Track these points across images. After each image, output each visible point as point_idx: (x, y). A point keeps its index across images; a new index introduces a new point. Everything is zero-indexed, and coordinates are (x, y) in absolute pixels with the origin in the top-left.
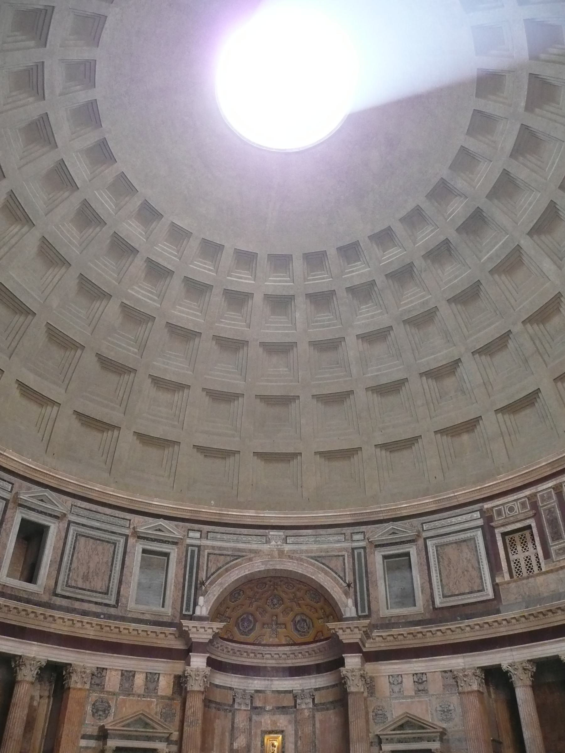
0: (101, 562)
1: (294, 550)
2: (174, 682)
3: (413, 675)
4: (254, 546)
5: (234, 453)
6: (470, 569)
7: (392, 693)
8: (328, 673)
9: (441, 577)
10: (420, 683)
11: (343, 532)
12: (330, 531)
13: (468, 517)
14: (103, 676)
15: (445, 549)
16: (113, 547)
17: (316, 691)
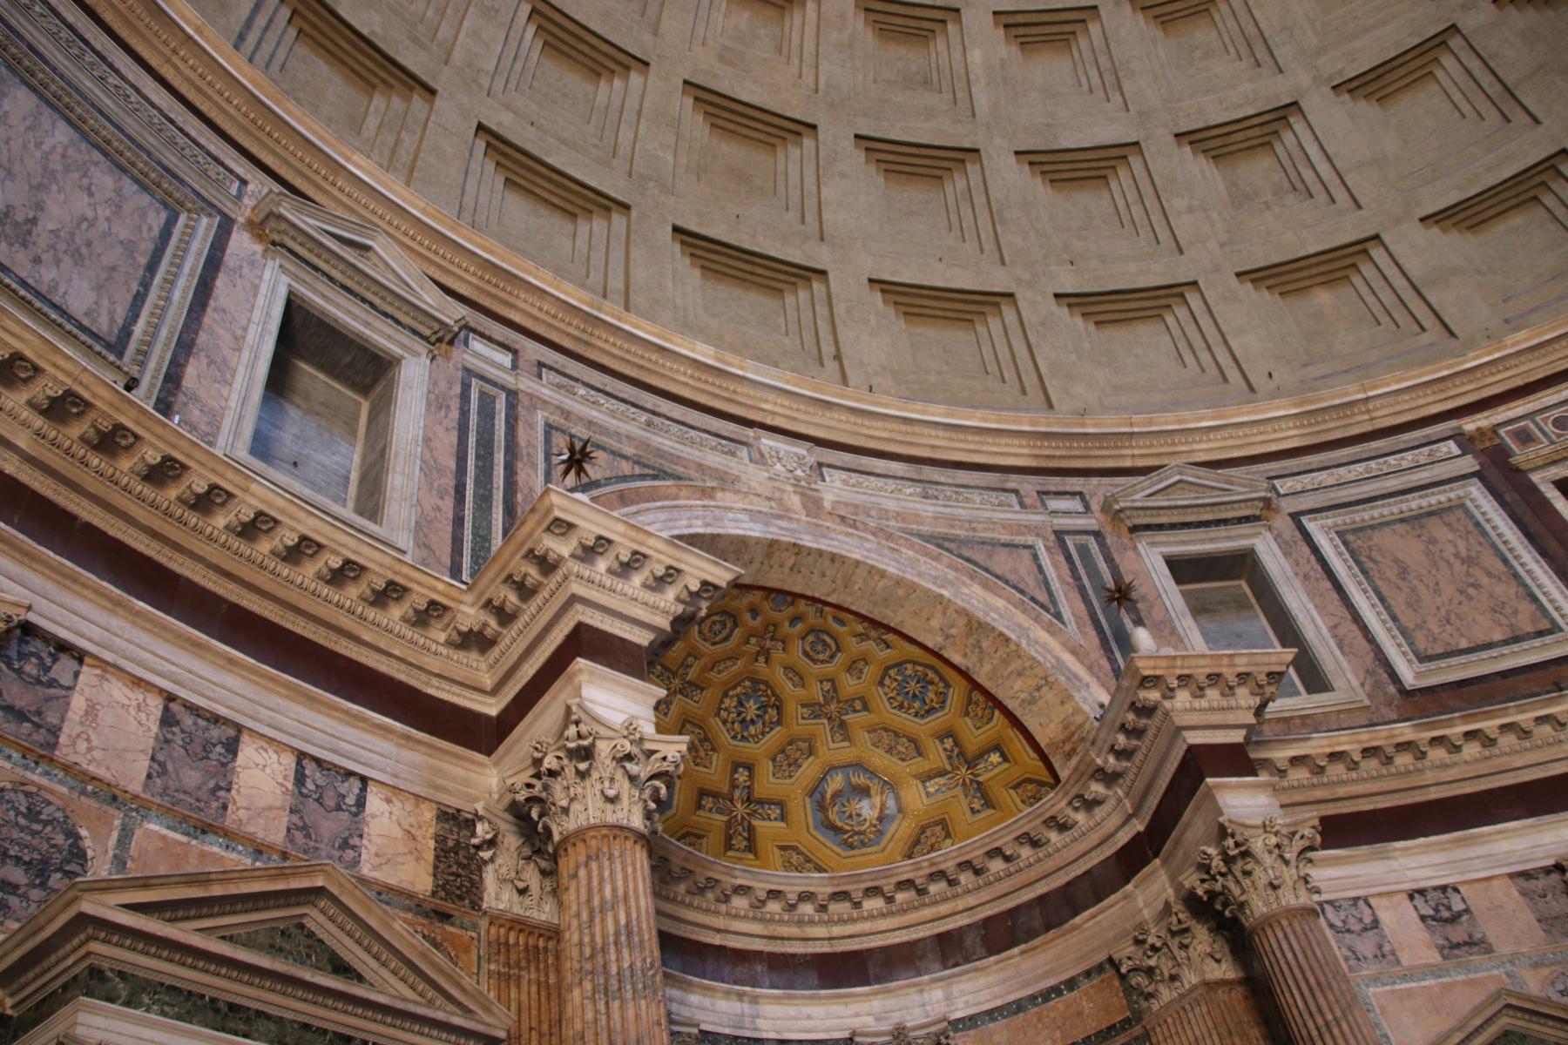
0: (103, 225)
1: (857, 506)
2: (440, 839)
3: (1411, 897)
4: (714, 459)
5: (608, 204)
6: (1485, 580)
7: (1353, 962)
8: (1016, 950)
9: (1388, 608)
10: (1446, 921)
11: (1011, 485)
12: (963, 476)
13: (1422, 455)
14: (53, 683)
15: (1370, 539)
16: (164, 215)
17: (956, 1030)
